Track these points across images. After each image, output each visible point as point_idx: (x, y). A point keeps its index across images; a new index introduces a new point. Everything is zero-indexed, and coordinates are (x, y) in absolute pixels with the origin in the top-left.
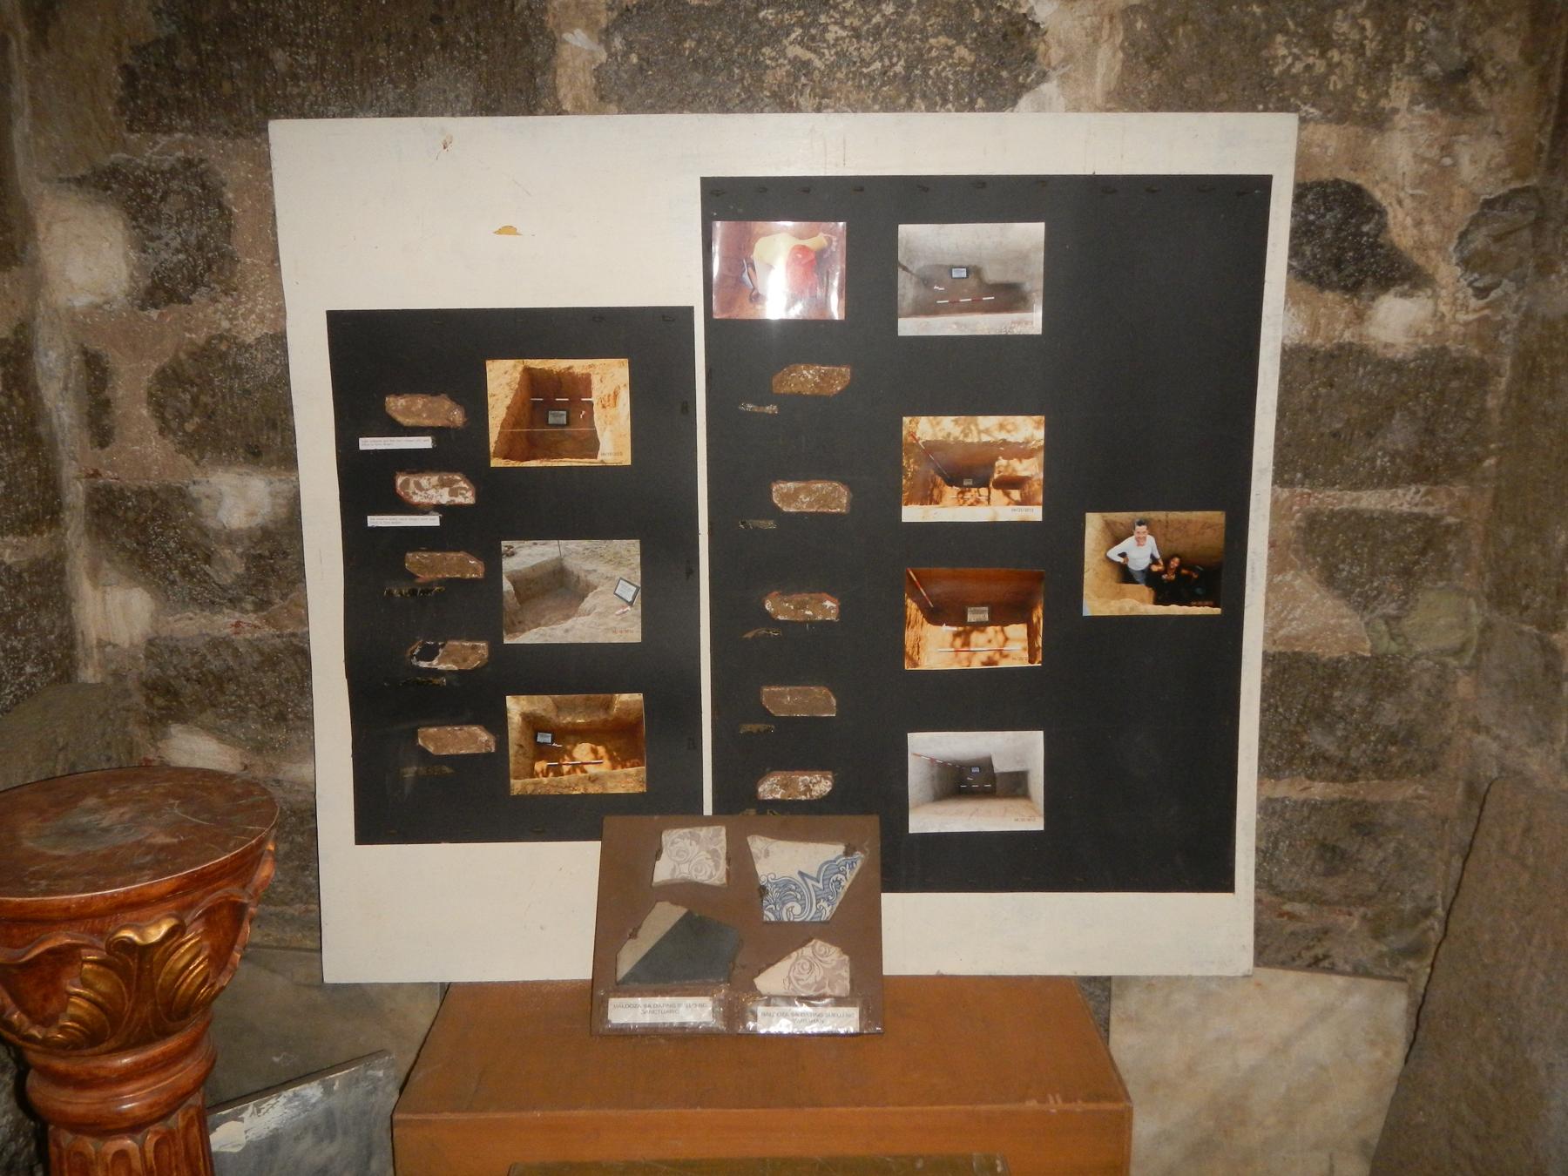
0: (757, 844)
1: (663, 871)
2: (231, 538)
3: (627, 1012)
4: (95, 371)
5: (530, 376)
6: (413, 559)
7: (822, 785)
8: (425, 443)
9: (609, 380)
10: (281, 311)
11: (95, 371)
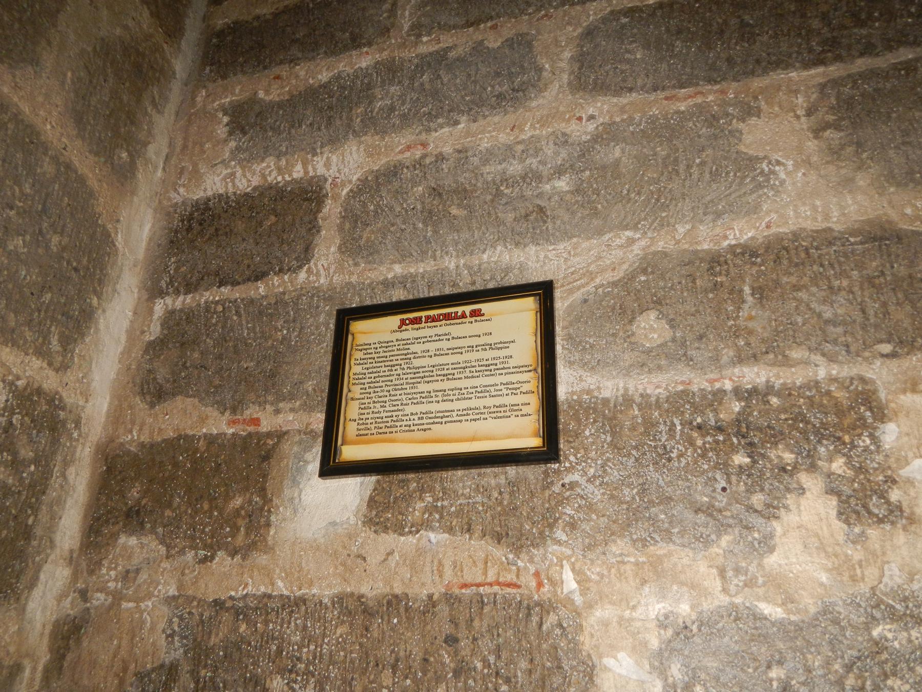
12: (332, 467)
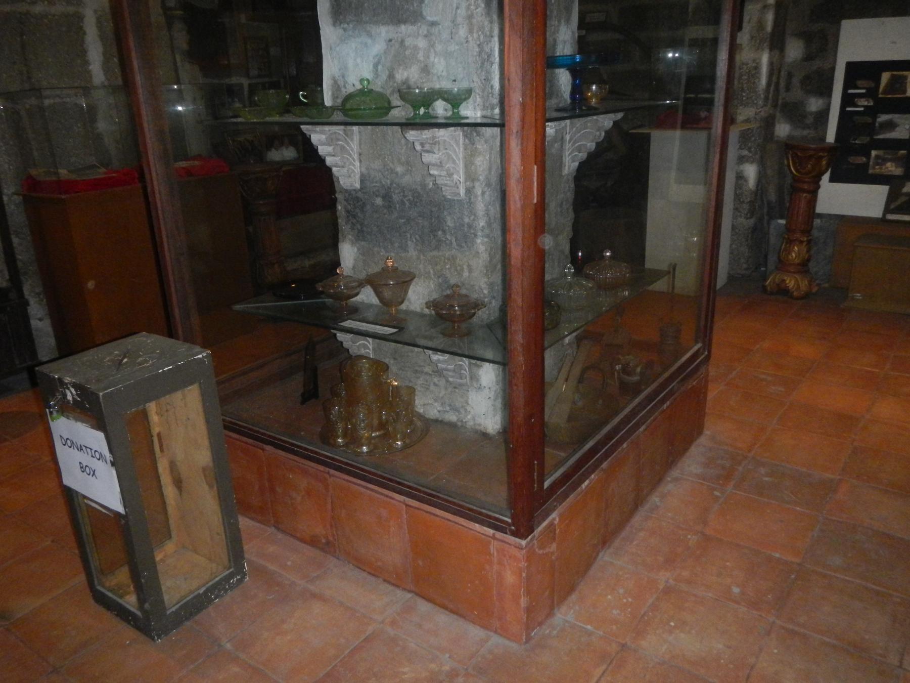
2: (811, 113)
3: (890, 217)
4: (790, 75)
5: (893, 76)
6: (856, 118)
8: (863, 91)
11: (790, 75)
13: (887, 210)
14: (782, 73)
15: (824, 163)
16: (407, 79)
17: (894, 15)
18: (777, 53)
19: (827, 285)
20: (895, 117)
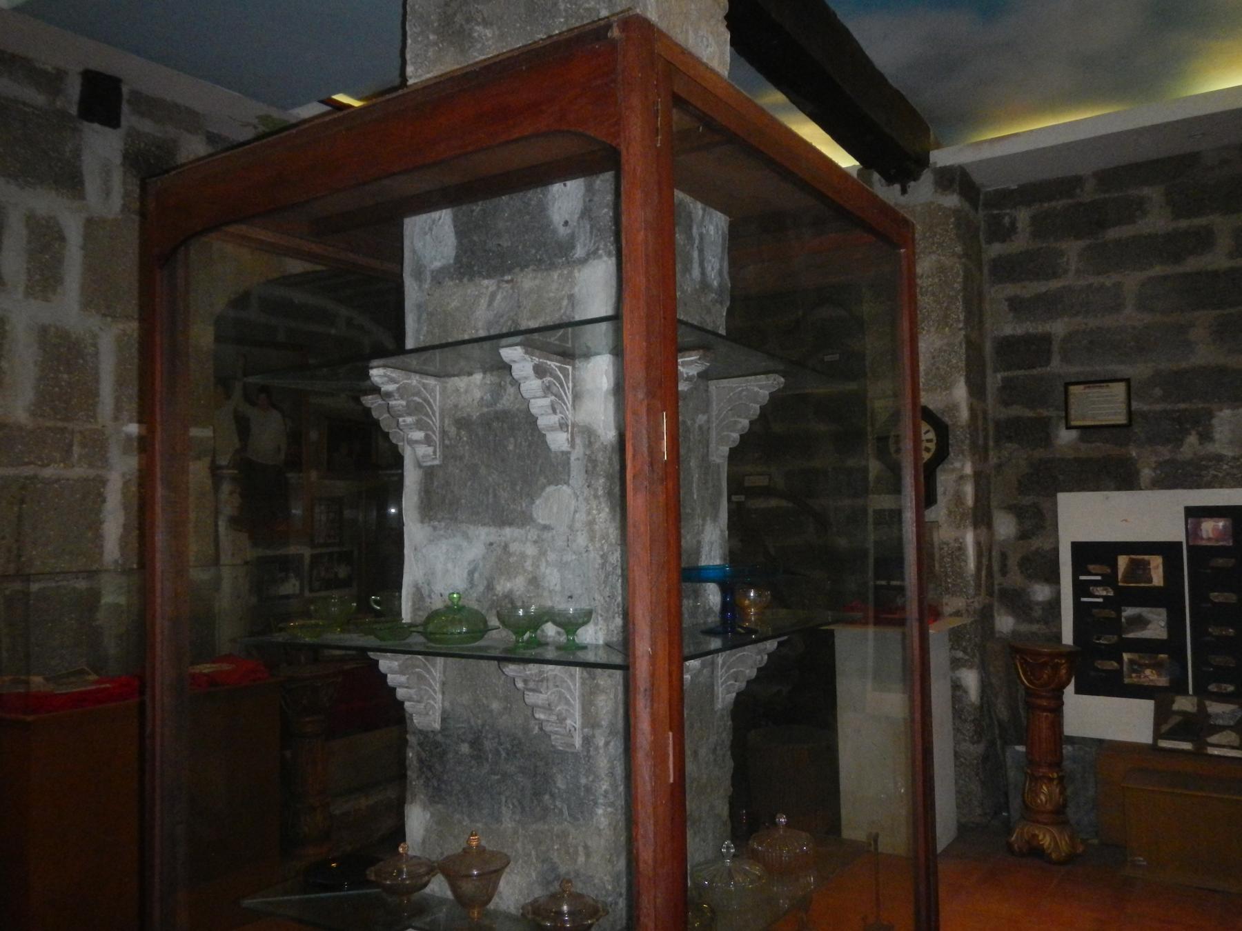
0: (1207, 703)
1: (1175, 707)
2: (1038, 603)
3: (1164, 744)
4: (1004, 556)
5: (1132, 561)
6: (1095, 611)
7: (1231, 688)
8: (1099, 578)
9: (1156, 564)
10: (1057, 542)
11: (1004, 556)
12: (1069, 427)
13: (1157, 735)
14: (994, 553)
15: (1064, 671)
16: (511, 591)
17: (1118, 489)
18: (983, 530)
19: (1095, 841)
20: (1145, 611)
